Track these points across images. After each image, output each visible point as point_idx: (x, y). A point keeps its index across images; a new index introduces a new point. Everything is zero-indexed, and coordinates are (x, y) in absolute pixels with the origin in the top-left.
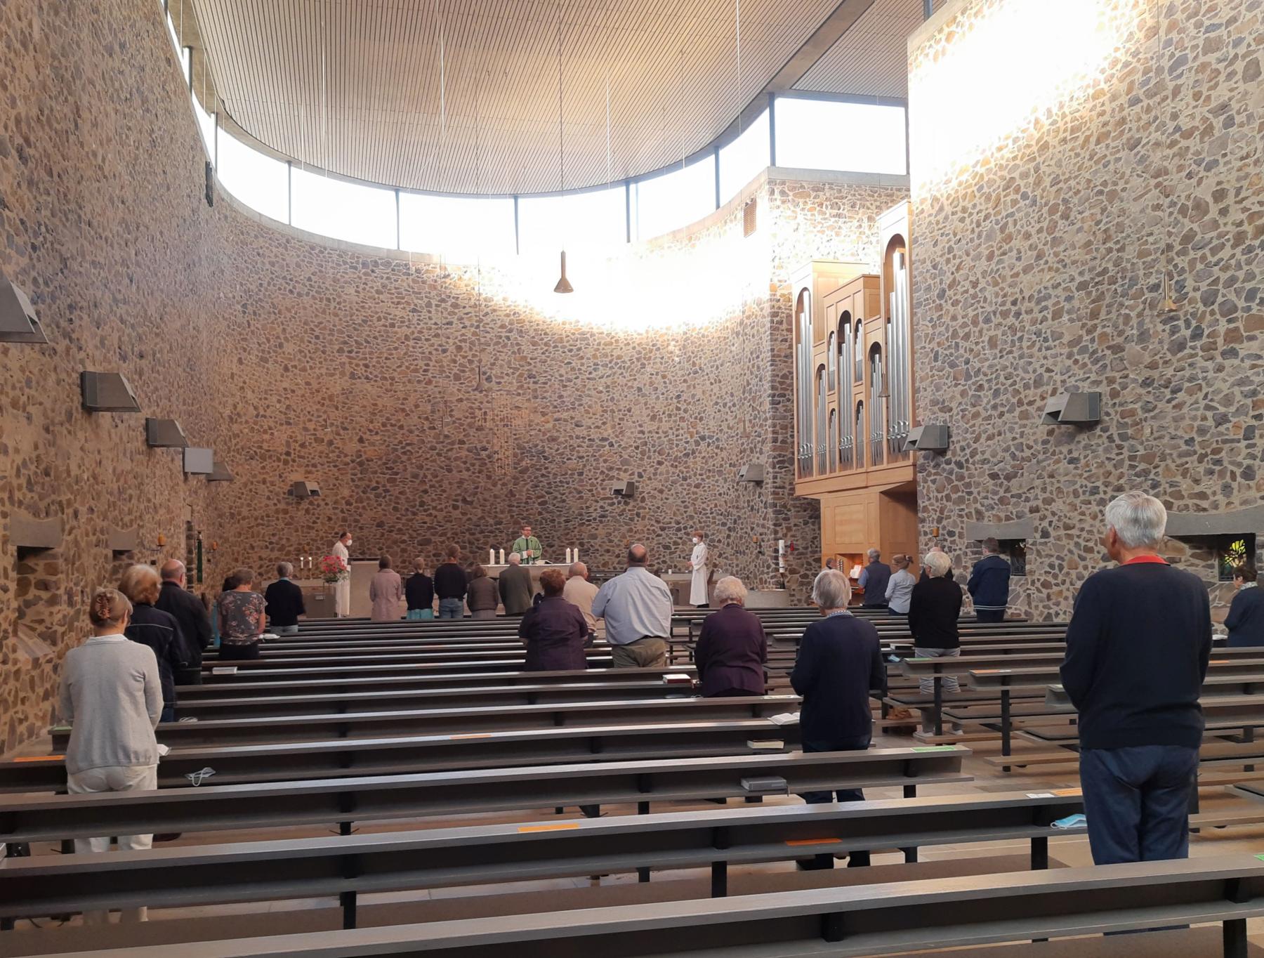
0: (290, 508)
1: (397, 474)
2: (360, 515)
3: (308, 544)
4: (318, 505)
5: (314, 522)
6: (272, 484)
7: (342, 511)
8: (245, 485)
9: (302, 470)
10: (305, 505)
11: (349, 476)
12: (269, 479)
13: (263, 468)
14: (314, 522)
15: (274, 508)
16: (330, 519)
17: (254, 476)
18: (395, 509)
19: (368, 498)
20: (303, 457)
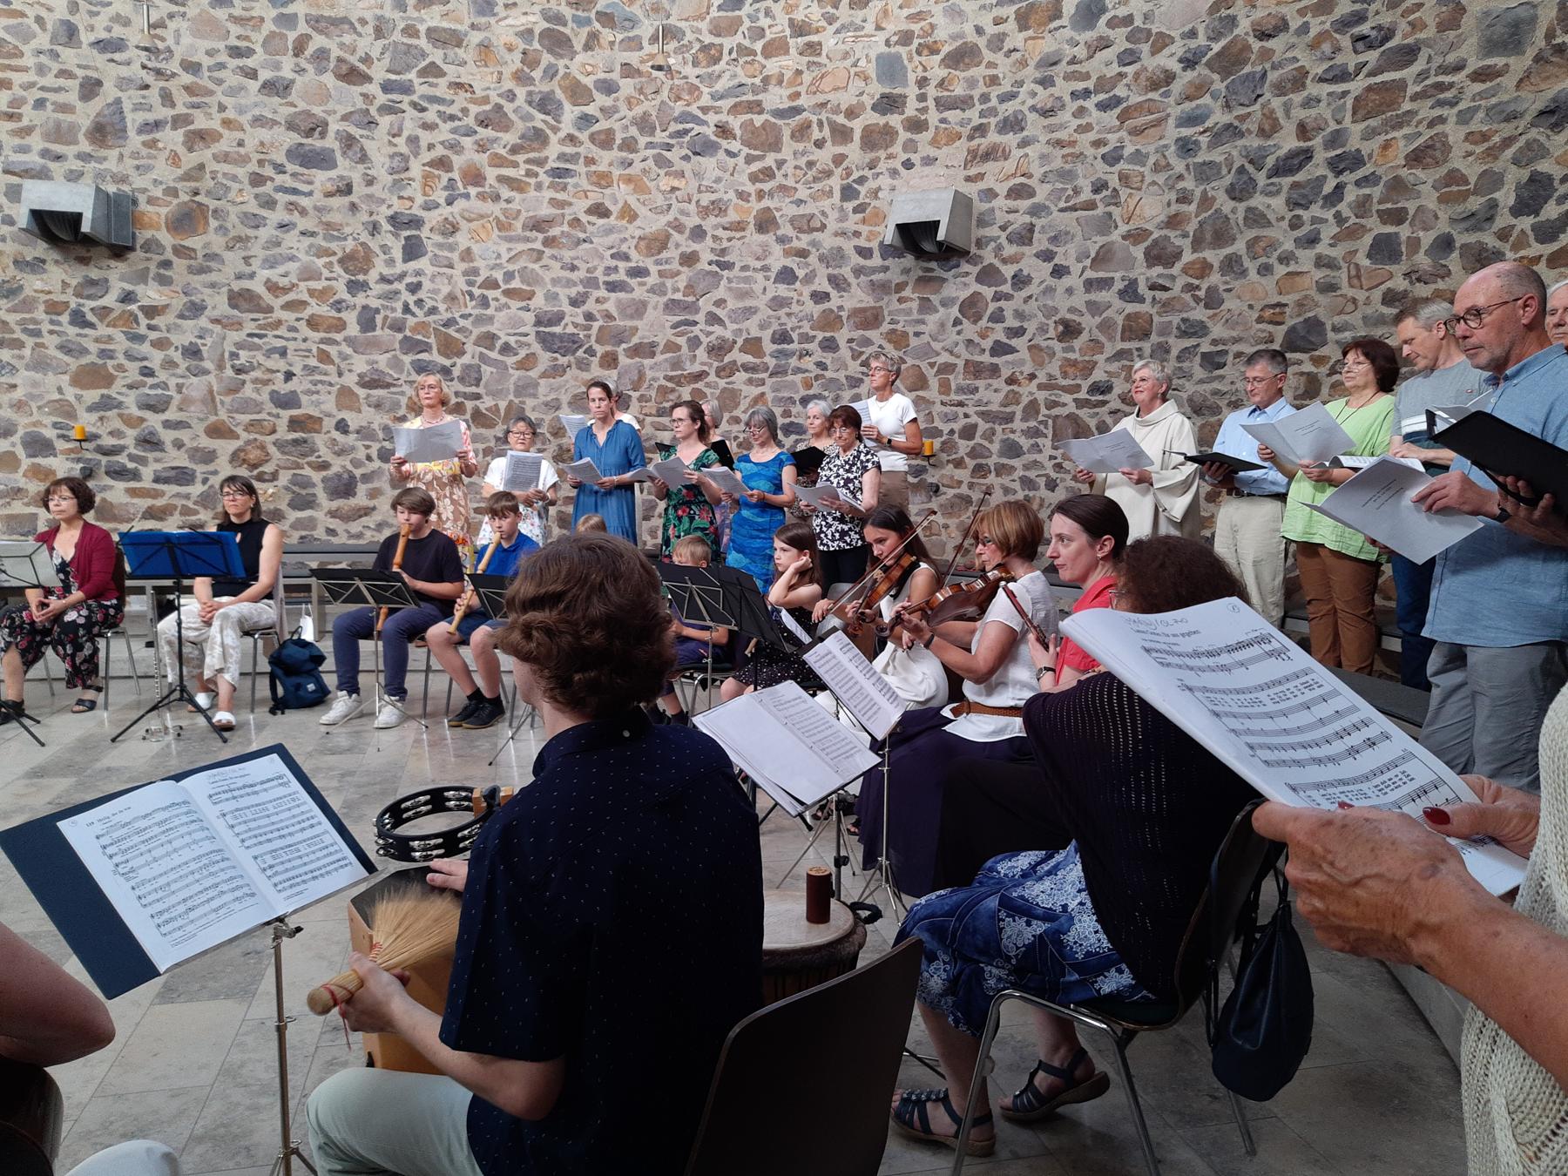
0: (890, 304)
1: (1408, 54)
2: (1212, 300)
3: (968, 432)
4: (1020, 281)
5: (1000, 349)
6: (806, 225)
7: (1130, 292)
8: (657, 244)
9: (960, 149)
10: (960, 285)
11: (1172, 132)
12: (785, 209)
13: (768, 174)
14: (1000, 349)
15: (817, 310)
16: (1069, 331)
17: (718, 208)
18: (1385, 250)
19: (1256, 218)
20: (964, 103)
